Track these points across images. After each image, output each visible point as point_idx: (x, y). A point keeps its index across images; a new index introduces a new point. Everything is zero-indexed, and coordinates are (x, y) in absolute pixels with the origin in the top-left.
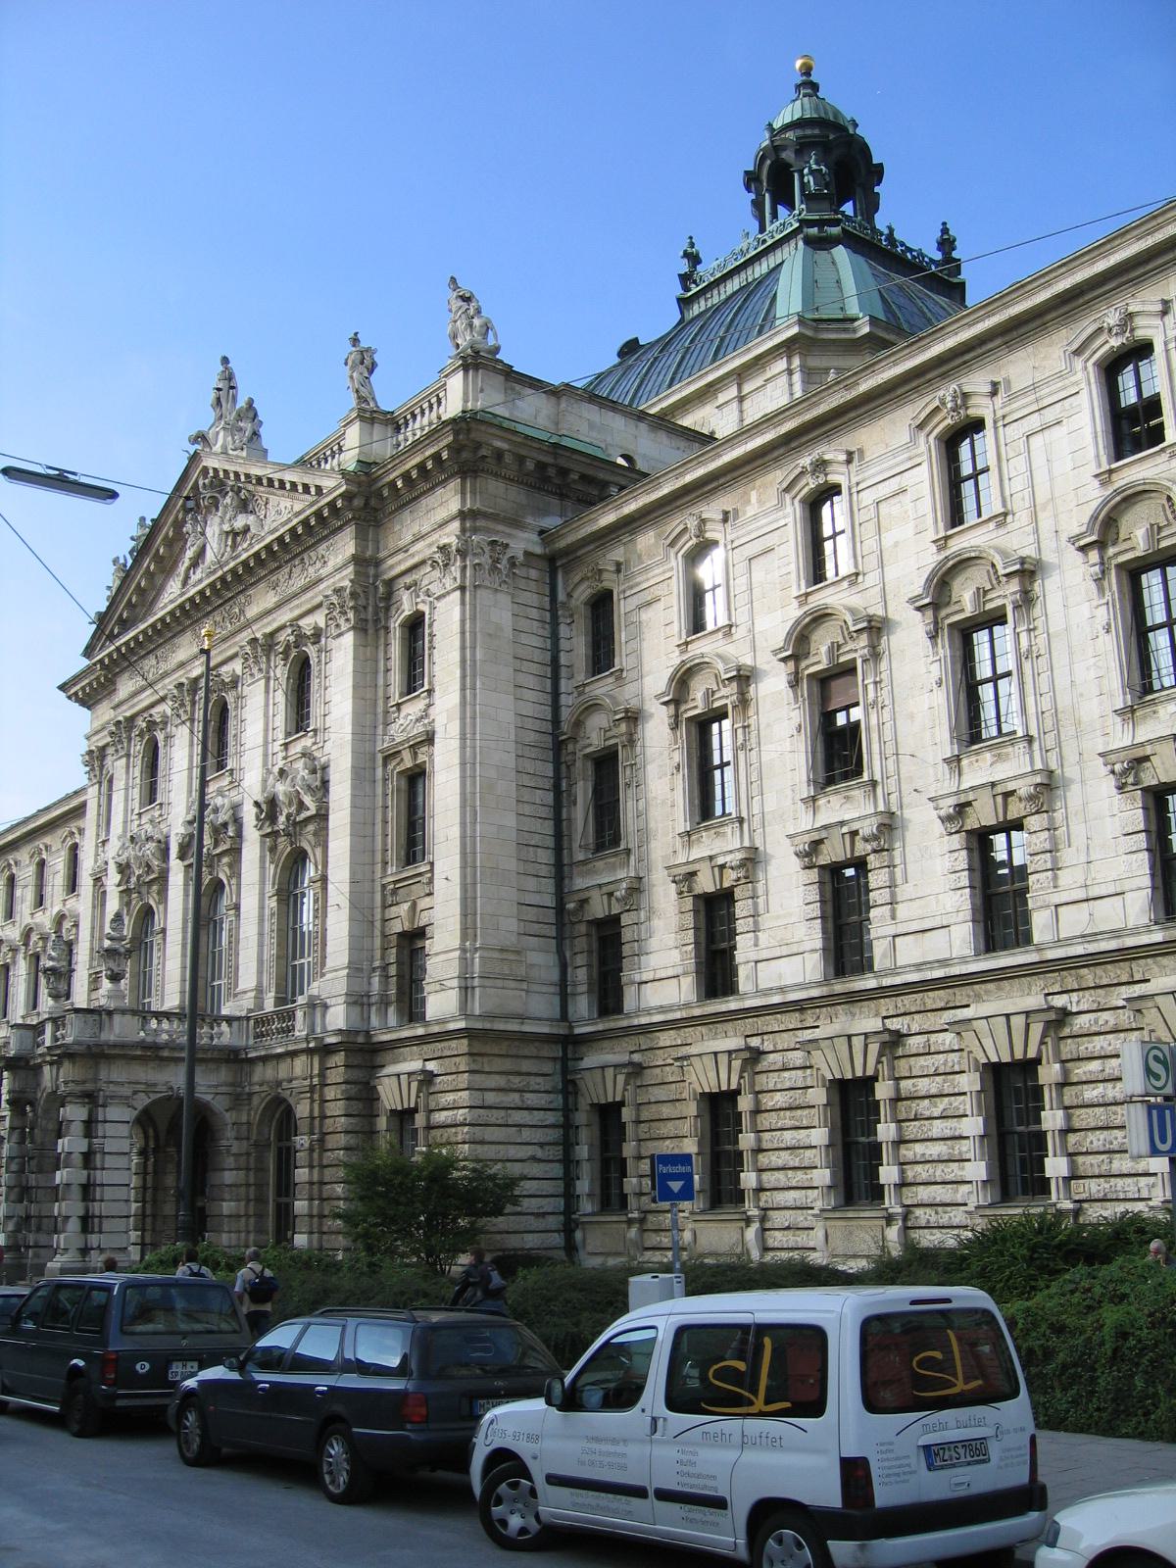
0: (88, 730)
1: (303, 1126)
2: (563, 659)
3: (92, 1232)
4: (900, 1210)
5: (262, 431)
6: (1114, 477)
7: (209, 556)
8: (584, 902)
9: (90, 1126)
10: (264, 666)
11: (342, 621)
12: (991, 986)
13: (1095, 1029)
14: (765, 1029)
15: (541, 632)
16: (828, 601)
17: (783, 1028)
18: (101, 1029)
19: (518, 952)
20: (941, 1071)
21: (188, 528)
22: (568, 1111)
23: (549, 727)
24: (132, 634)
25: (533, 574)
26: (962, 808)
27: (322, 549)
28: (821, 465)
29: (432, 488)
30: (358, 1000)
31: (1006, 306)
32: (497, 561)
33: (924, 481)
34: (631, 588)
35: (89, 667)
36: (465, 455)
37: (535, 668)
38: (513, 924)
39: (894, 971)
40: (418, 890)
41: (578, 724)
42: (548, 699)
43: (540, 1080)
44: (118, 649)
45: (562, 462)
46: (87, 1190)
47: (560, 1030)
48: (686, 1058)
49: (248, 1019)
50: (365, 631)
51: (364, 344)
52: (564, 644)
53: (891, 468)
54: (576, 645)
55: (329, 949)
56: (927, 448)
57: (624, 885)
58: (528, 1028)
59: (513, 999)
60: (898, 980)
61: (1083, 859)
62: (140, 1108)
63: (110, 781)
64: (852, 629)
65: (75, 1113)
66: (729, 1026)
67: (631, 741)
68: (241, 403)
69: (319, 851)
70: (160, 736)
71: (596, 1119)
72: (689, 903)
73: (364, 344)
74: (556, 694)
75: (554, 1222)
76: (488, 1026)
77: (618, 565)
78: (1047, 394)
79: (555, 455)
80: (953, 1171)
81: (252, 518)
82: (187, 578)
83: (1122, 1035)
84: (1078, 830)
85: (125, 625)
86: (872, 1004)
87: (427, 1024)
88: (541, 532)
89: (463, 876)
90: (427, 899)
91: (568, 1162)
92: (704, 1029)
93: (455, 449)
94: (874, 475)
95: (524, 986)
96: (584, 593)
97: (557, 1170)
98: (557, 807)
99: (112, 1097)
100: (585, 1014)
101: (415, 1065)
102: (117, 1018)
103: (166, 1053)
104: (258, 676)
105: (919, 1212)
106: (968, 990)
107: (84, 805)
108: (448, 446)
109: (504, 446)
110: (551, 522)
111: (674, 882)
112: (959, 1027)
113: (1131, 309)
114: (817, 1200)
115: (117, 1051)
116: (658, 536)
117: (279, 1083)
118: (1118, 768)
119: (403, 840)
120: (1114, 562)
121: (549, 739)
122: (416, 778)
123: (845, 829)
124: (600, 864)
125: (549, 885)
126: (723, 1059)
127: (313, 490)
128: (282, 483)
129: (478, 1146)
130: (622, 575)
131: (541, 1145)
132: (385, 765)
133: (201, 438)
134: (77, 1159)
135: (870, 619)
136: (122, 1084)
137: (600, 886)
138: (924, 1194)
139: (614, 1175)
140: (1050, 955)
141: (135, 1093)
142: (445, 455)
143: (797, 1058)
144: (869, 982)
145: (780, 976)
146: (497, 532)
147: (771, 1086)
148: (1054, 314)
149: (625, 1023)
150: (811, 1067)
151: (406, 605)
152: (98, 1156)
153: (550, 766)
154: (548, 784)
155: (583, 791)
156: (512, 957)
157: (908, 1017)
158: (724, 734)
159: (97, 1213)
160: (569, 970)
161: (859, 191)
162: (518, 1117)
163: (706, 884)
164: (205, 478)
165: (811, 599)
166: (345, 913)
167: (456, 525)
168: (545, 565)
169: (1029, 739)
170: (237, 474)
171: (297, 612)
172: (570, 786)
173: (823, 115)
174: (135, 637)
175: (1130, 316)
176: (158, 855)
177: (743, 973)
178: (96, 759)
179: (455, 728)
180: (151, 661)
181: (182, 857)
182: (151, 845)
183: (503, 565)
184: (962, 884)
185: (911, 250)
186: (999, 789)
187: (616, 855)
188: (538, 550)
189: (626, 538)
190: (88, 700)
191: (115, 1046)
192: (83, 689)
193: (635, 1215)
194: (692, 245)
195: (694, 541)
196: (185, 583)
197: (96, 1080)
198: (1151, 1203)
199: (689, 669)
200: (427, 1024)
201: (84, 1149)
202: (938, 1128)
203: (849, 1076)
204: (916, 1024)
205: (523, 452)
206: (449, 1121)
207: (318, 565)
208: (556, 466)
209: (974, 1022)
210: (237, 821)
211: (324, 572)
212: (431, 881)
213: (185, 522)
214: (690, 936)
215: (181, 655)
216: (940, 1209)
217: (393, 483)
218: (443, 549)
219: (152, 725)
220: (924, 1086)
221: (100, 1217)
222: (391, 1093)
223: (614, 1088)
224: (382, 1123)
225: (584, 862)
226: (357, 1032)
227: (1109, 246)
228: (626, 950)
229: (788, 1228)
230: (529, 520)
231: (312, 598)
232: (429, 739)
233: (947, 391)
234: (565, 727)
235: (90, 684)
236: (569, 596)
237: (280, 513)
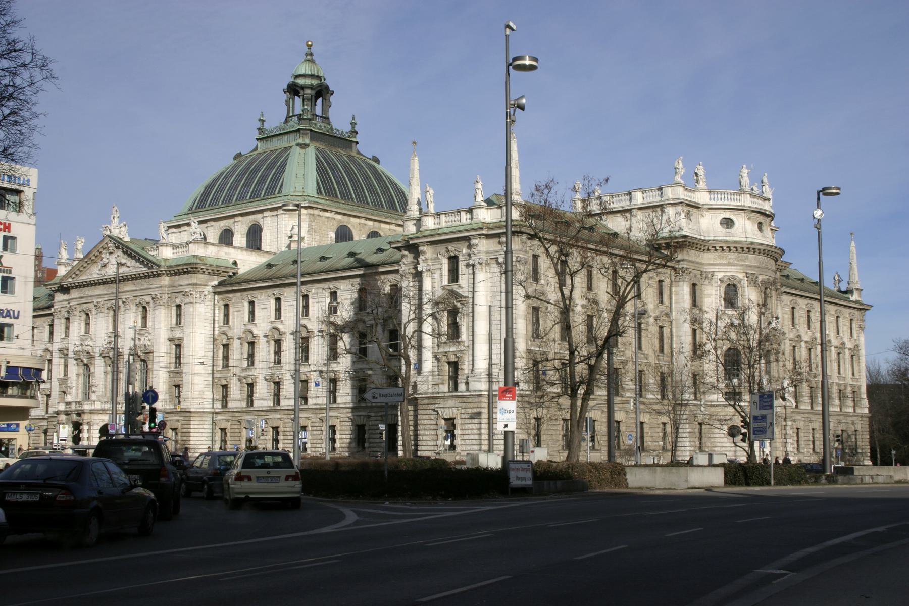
2: (216, 319)
9: (89, 431)
37: (209, 321)
39: (283, 406)
47: (213, 410)
52: (217, 315)
54: (220, 316)
58: (205, 410)
74: (214, 327)
124: (223, 372)
131: (207, 437)
134: (86, 439)
149: (228, 410)
154: (211, 350)
173: (313, 73)
185: (338, 130)
234: (216, 336)
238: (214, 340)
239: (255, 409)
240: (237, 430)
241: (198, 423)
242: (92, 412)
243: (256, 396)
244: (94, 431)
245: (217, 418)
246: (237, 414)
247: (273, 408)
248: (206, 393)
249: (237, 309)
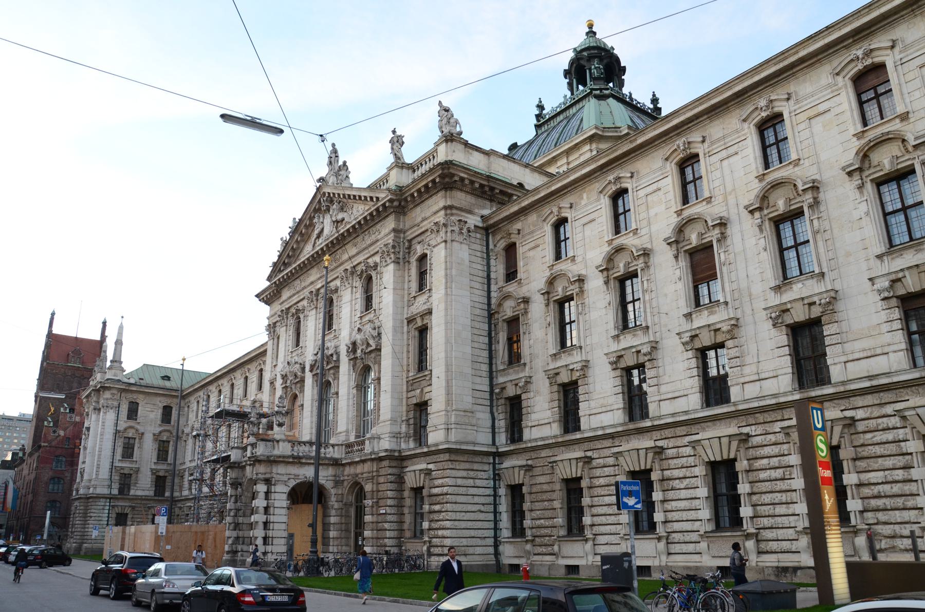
0: (268, 315)
1: (368, 495)
2: (493, 275)
3: (269, 545)
4: (665, 534)
5: (350, 176)
6: (766, 177)
7: (326, 232)
8: (503, 389)
9: (267, 494)
10: (350, 282)
11: (388, 259)
12: (709, 424)
13: (765, 443)
14: (594, 447)
15: (482, 263)
16: (623, 242)
17: (603, 446)
18: (274, 448)
19: (472, 412)
20: (685, 466)
21: (316, 220)
22: (495, 489)
23: (486, 307)
24: (289, 269)
25: (478, 236)
26: (693, 337)
27: (378, 226)
28: (618, 179)
30: (396, 436)
31: (710, 99)
32: (461, 229)
33: (670, 184)
34: (525, 241)
35: (269, 286)
36: (447, 180)
37: (479, 279)
38: (470, 399)
39: (660, 418)
40: (424, 383)
41: (500, 305)
42: (485, 294)
43: (482, 473)
44: (283, 277)
45: (492, 185)
46: (266, 524)
47: (494, 450)
48: (555, 462)
49: (342, 445)
50: (398, 263)
51: (398, 133)
52: (493, 269)
53: (654, 179)
54: (499, 269)
55: (381, 412)
56: (672, 169)
57: (523, 380)
59: (471, 435)
60: (662, 422)
61: (756, 360)
62: (291, 486)
63: (278, 338)
64: (635, 254)
65: (261, 488)
66: (576, 446)
67: (526, 312)
68: (341, 163)
69: (376, 366)
70: (302, 316)
71: (509, 492)
72: (555, 388)
73: (398, 133)
74: (489, 292)
75: (491, 541)
76: (458, 447)
77: (519, 230)
78: (730, 141)
79: (488, 181)
80: (692, 515)
81: (346, 214)
82: (315, 243)
83: (779, 446)
84: (753, 348)
85: (286, 265)
86: (649, 434)
87: (428, 446)
88: (482, 217)
89: (447, 376)
90: (429, 387)
91: (496, 512)
92: (563, 448)
93: (442, 176)
94: (644, 183)
95: (475, 428)
96: (502, 244)
97: (491, 516)
98: (490, 344)
99: (278, 481)
100: (504, 442)
101: (423, 466)
102: (281, 443)
103: (304, 461)
104: (347, 286)
105: (674, 535)
106: (698, 426)
107: (266, 351)
108: (439, 176)
109: (465, 176)
110: (486, 212)
111: (548, 378)
112: (694, 444)
113: (772, 98)
114: (623, 530)
115: (281, 459)
116: (538, 216)
117: (357, 475)
118: (773, 315)
119: (417, 361)
120: (767, 217)
121: (486, 312)
122: (423, 331)
123: (634, 350)
124: (511, 371)
125: (487, 381)
126: (574, 462)
127: (375, 199)
128: (360, 197)
129: (454, 505)
130: (521, 235)
131: (483, 504)
132: (408, 325)
133: (321, 180)
134: (262, 510)
135: (644, 250)
136: (283, 475)
137: (511, 381)
138: (677, 526)
139: (518, 519)
140: (741, 407)
141: (289, 479)
142: (437, 180)
143: (611, 461)
144: (648, 423)
145: (602, 422)
146: (462, 216)
147: (598, 475)
148: (733, 103)
149: (524, 446)
150: (618, 465)
151: (419, 250)
152: (272, 509)
153: (487, 325)
154: (486, 333)
155: (502, 337)
156: (470, 414)
157: (667, 440)
158: (571, 310)
159: (271, 536)
160: (496, 421)
161: (616, 78)
162: (472, 491)
163: (564, 378)
164: (324, 196)
165: (614, 242)
166: (389, 395)
167: (443, 212)
168: (483, 232)
169: (726, 303)
170: (339, 195)
171: (366, 256)
172: (496, 334)
174: (291, 271)
175: (771, 101)
176: (300, 370)
177: (583, 421)
178: (272, 328)
179: (442, 306)
180: (298, 282)
181: (311, 371)
182: (298, 366)
183: (465, 231)
184: (694, 375)
185: (639, 103)
186: (712, 328)
187: (519, 366)
188: (481, 225)
189: (522, 218)
190: (268, 302)
191: (280, 457)
192: (266, 296)
193: (530, 538)
194: (541, 102)
195: (556, 218)
196: (314, 246)
197: (271, 473)
198: (797, 529)
199: (555, 277)
200: (428, 446)
201: (265, 505)
202: (684, 494)
203: (637, 469)
204: (671, 443)
205: (474, 179)
206: (440, 493)
207: (377, 233)
208: (488, 186)
209: (702, 442)
210: (338, 354)
211: (379, 237)
212: (431, 379)
213: (314, 217)
214: (556, 404)
215: (312, 278)
216: (685, 534)
217: (412, 195)
218: (436, 224)
219: (298, 311)
220: (677, 473)
221: (272, 537)
222: (411, 480)
223: (518, 477)
224: (406, 494)
225: (504, 370)
226: (395, 451)
227: (760, 69)
228: (524, 411)
229: (607, 544)
230: (476, 211)
232: (430, 312)
233: (680, 142)
234: (493, 307)
235: (270, 294)
236: (495, 246)
237: (359, 211)
238: (491, 316)
239: (586, 435)
240: (545, 487)
241: (464, 474)
242: (271, 461)
243: (584, 409)
244: (277, 496)
245: (504, 466)
246: (544, 453)
247: (631, 426)
248: (479, 415)
249: (532, 245)
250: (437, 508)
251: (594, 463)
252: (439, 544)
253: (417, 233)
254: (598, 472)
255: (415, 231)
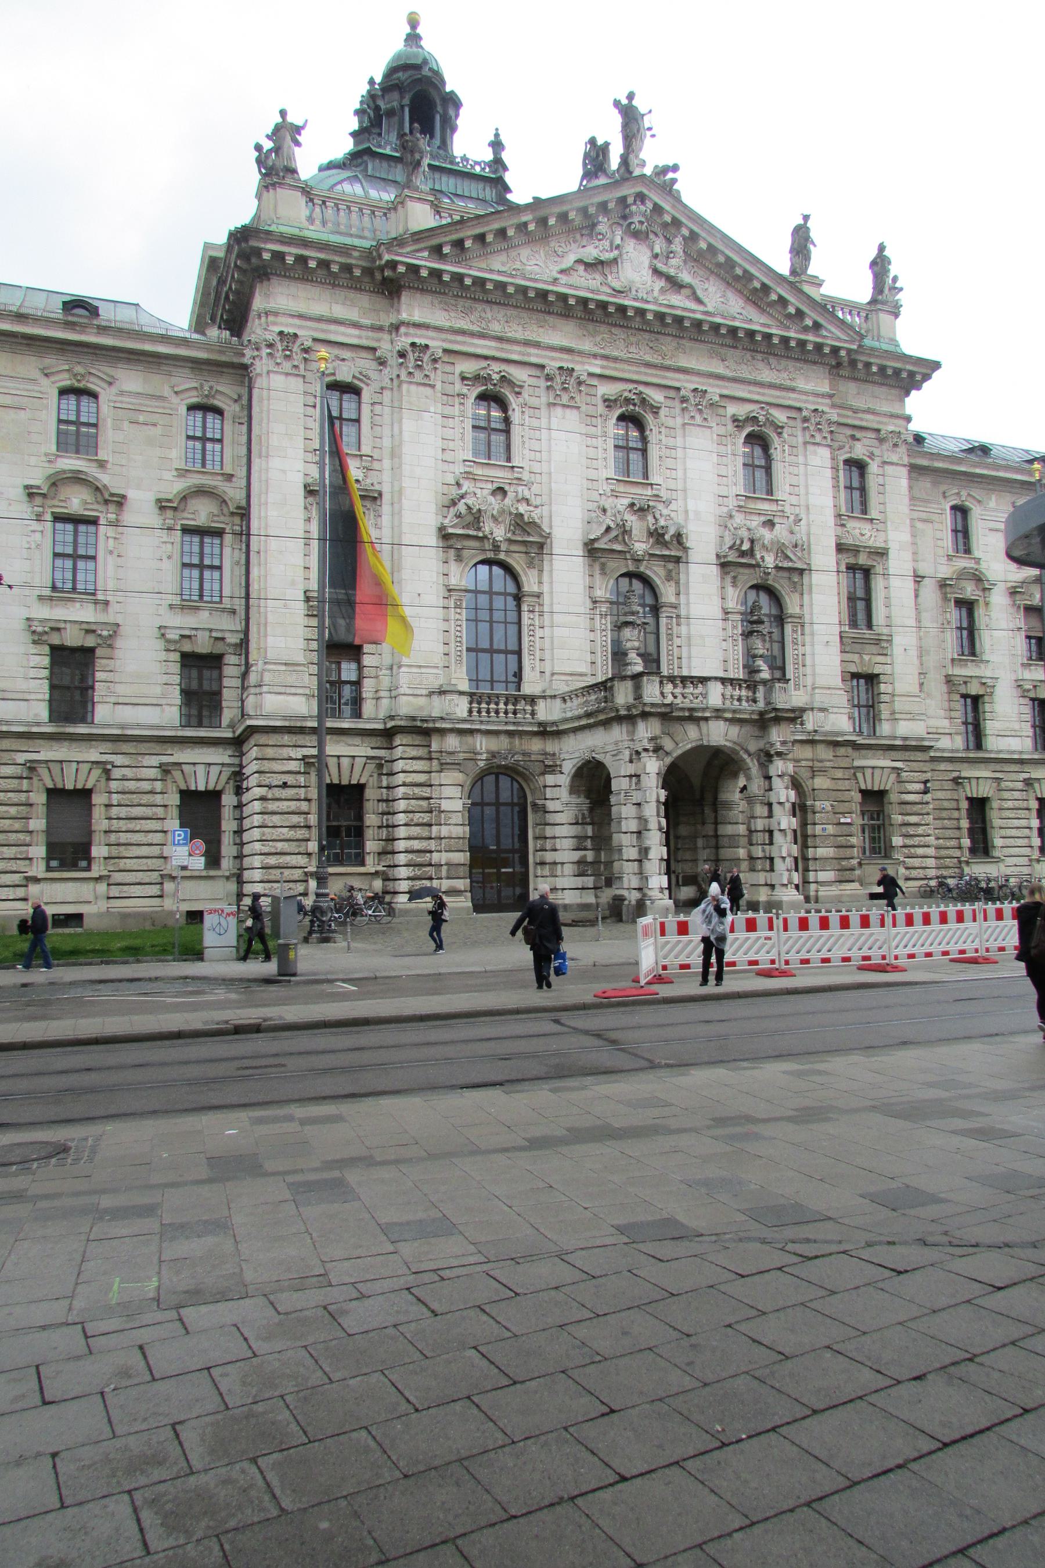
29: (883, 384)
66: (982, 765)
217: (868, 365)
231: (778, 397)
243: (990, 727)
246: (943, 766)
249: (924, 516)
250: (913, 819)
251: (1003, 785)
252: (917, 865)
253: (850, 421)
254: (1006, 795)
255: (847, 417)
